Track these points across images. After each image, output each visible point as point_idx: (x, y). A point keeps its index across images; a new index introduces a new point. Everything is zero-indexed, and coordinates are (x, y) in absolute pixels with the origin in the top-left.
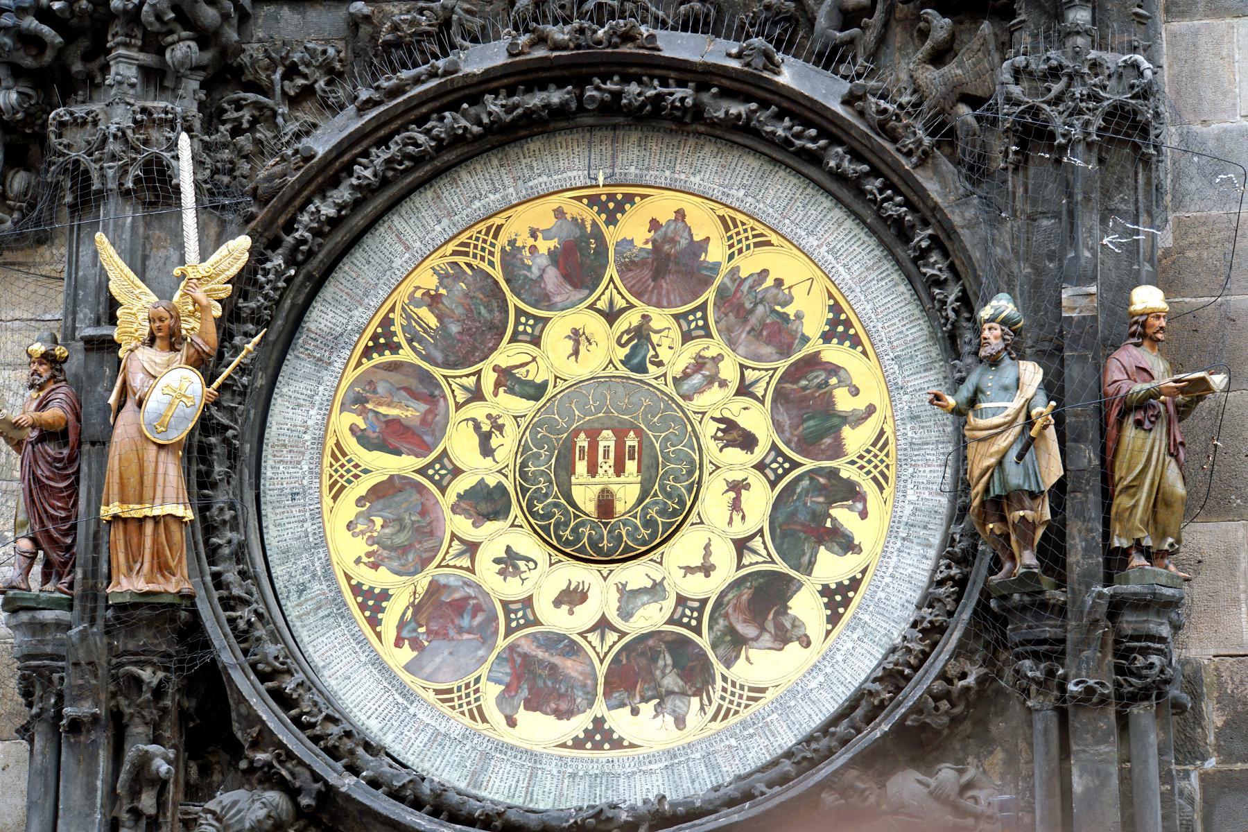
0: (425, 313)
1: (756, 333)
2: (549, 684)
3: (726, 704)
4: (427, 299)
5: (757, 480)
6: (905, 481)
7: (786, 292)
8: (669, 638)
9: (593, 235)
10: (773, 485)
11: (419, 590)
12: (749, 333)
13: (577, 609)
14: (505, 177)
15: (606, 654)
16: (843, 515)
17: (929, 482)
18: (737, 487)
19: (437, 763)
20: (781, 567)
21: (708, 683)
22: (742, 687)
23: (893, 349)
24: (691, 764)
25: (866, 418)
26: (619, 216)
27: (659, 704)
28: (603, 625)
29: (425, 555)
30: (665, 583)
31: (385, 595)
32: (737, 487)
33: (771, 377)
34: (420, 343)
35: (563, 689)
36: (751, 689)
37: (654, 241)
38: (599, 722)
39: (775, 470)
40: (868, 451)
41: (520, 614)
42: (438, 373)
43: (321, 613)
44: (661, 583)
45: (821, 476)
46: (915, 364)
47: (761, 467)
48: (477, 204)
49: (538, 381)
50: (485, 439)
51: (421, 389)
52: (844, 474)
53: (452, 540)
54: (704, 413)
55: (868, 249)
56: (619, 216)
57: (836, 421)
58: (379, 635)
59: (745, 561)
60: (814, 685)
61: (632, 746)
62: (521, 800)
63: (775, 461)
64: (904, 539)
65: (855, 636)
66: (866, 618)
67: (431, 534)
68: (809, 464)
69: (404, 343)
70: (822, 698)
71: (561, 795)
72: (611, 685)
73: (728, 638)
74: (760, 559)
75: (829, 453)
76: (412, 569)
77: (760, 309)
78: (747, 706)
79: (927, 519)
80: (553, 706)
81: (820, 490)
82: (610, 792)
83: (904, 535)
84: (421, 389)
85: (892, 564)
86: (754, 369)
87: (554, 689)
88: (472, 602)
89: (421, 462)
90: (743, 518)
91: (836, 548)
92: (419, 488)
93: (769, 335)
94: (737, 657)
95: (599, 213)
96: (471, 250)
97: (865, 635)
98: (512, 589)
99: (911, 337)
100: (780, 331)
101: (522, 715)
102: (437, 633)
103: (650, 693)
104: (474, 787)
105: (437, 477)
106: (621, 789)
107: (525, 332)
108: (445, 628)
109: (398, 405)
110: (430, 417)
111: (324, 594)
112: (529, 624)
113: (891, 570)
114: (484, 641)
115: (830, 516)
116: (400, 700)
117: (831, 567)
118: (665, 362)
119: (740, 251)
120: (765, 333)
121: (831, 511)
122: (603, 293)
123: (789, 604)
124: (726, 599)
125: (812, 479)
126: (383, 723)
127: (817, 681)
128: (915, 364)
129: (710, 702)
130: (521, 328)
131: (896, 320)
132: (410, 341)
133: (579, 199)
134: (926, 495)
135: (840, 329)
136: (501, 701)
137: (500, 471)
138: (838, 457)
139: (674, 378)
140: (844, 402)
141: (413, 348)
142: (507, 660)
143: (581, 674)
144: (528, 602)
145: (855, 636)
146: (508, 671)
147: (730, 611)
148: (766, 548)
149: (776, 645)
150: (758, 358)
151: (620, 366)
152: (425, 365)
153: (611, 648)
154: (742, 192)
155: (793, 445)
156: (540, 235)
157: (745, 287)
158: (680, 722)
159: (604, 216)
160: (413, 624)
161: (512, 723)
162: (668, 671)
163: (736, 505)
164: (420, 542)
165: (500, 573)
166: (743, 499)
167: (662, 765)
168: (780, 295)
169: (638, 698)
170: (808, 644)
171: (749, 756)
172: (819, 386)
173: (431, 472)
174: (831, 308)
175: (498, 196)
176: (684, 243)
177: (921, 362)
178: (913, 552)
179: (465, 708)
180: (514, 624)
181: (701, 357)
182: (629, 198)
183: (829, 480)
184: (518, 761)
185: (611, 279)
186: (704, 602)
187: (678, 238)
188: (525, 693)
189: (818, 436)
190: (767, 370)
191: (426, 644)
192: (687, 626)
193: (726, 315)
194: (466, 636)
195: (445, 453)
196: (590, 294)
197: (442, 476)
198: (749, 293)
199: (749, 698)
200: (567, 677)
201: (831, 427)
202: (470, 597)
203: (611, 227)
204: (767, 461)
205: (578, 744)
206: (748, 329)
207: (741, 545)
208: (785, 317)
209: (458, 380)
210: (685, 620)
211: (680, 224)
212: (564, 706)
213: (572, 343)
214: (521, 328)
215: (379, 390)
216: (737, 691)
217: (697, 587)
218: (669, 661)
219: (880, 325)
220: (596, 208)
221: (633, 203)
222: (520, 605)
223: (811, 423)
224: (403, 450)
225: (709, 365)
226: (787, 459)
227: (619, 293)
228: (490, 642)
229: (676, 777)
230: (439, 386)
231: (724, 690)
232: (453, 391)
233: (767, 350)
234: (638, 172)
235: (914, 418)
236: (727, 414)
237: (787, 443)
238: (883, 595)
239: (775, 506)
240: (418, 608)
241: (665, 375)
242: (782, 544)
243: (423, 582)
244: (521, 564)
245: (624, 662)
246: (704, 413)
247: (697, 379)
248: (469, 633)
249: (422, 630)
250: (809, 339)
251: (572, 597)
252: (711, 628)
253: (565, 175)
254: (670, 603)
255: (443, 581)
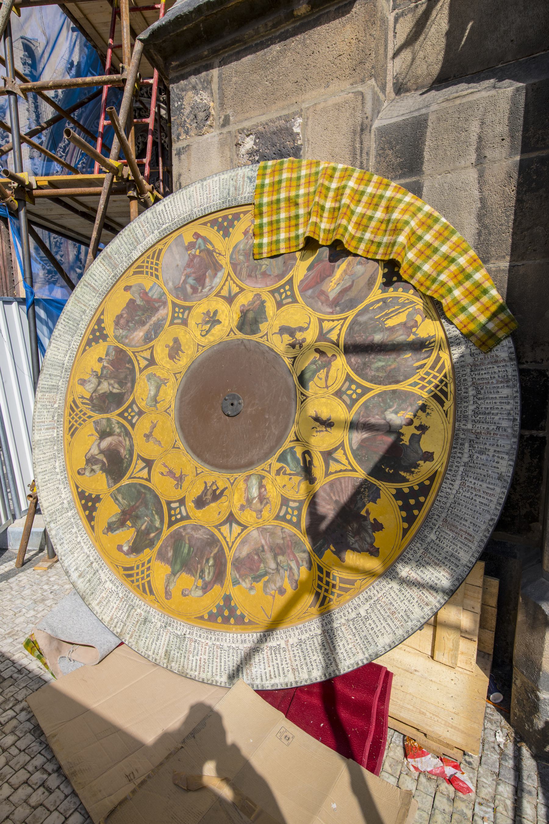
0: (402, 318)
1: (259, 551)
2: (137, 318)
3: (77, 411)
4: (412, 323)
5: (177, 494)
6: (117, 587)
7: (273, 592)
8: (126, 397)
9: (396, 474)
10: (169, 503)
11: (221, 257)
12: (263, 547)
13: (167, 351)
14: (486, 426)
15: (136, 357)
16: (126, 536)
17: (109, 601)
18: (180, 480)
19: (124, 238)
20: (125, 481)
21: (93, 407)
22: (80, 424)
23: (191, 640)
24: (58, 378)
25: (166, 589)
26: (400, 503)
27: (97, 375)
28: (152, 362)
29: (239, 268)
30: (154, 408)
31: (226, 234)
32: (180, 480)
33: (227, 542)
34: (380, 308)
35: (130, 325)
36: (76, 429)
37: (365, 518)
38: (105, 337)
39: (175, 509)
40: (148, 576)
41: (181, 316)
42: (351, 314)
43: (232, 189)
44: (155, 406)
45: (155, 536)
46: (174, 647)
47: (182, 502)
48: (471, 392)
49: (311, 384)
50: (291, 332)
51: (346, 298)
52: (147, 551)
53: (240, 288)
54: (232, 484)
55: (264, 677)
56: (400, 503)
57: (178, 567)
58: (205, 224)
59: (140, 461)
60: (57, 464)
61: (85, 350)
62: (87, 279)
63: (180, 513)
64: (92, 563)
65: (65, 502)
66: (70, 514)
67: (250, 276)
68: (166, 533)
69: (385, 295)
70: (49, 465)
71: (79, 302)
72: (120, 352)
73: (108, 430)
74: (135, 471)
75: (164, 549)
76: (234, 256)
77: (273, 565)
78: (70, 422)
79: (92, 585)
80: (125, 316)
81: (148, 530)
82: (67, 328)
83: (94, 565)
84: (346, 298)
85: (85, 547)
86: (239, 534)
87: (133, 320)
88: (200, 288)
89: (296, 283)
90: (162, 474)
91: (114, 519)
92: (281, 276)
93: (253, 559)
94: (96, 429)
95: (411, 488)
96: (434, 373)
97: (62, 508)
98: (196, 316)
99: (191, 658)
100: (251, 569)
101: (128, 296)
102: (192, 261)
103: (105, 372)
104: (104, 256)
105: (282, 291)
106: (66, 335)
107: (349, 388)
108: (192, 267)
109: (342, 278)
110: (323, 298)
111: (242, 194)
112: (173, 318)
113: (82, 544)
114: (176, 288)
115: (132, 527)
116: (164, 226)
117: (109, 510)
118: (277, 477)
119: (320, 579)
120: (256, 557)
121: (134, 529)
122: (347, 459)
123: (104, 474)
124: (127, 439)
125: (157, 529)
126: (158, 213)
127: (58, 467)
128: (174, 647)
129: (83, 403)
130: (354, 387)
131: (207, 657)
132: (384, 300)
133: (432, 479)
134: (103, 594)
135: (226, 613)
136: (140, 286)
137: (267, 334)
138: (158, 554)
139: (263, 477)
140: (185, 580)
141: (378, 301)
142: (160, 298)
143: (133, 338)
144: (185, 323)
145: (65, 502)
146: (154, 297)
147: (120, 439)
148: (139, 478)
149: (89, 455)
150: (243, 542)
151: (292, 445)
152: (361, 307)
153: (138, 361)
154: (363, 613)
155: (182, 530)
156: (418, 433)
157: (293, 565)
158: (83, 382)
159: (406, 491)
160: (203, 247)
161: (127, 288)
162: (111, 388)
163: (171, 473)
164: (248, 267)
165: (208, 312)
166: (172, 480)
167: (66, 362)
168: (274, 587)
169: (106, 364)
170: (79, 473)
171: (45, 411)
172: (202, 571)
173: (287, 287)
174: (242, 617)
175: (470, 413)
176: (352, 540)
177: (172, 652)
178: (83, 564)
179: (145, 264)
180: (177, 310)
181: (267, 503)
182: (410, 519)
183: (150, 539)
184: (105, 284)
185: (354, 470)
186: (133, 426)
187: (357, 538)
188: (139, 302)
189: (177, 550)
190: (233, 543)
191: (189, 252)
192: (126, 410)
193: (283, 538)
194: (183, 278)
195: (295, 301)
196: (351, 448)
197: (281, 294)
198: (289, 565)
199: (73, 425)
200: (135, 329)
201: (176, 562)
202: (203, 287)
203: (394, 492)
204: (183, 508)
205: (100, 321)
206: (266, 547)
207: (149, 463)
208: (257, 579)
209: (339, 327)
210: (130, 410)
211: (367, 546)
212: (122, 321)
213: (324, 419)
214: (354, 387)
215: (359, 267)
216: (80, 421)
217: (143, 425)
218: (115, 391)
219: (210, 644)
220: (416, 488)
221: (404, 520)
222: (185, 317)
223: (186, 551)
224: (310, 273)
225: (259, 506)
226: (177, 521)
227: (341, 471)
228: (174, 291)
229: (56, 367)
230: (342, 311)
231: (85, 414)
232: (333, 321)
233: (245, 552)
234: (428, 540)
235: (146, 620)
236: (223, 498)
237: (184, 527)
238: (74, 531)
239: (156, 496)
240: (210, 253)
241: (269, 472)
242: (135, 488)
243: (224, 261)
244: (207, 327)
245: (127, 365)
246: (232, 484)
247: (255, 492)
248: (184, 281)
249: (197, 253)
250: (234, 585)
251: (175, 350)
252: (118, 423)
253: (459, 477)
254: (142, 404)
255: (220, 274)
